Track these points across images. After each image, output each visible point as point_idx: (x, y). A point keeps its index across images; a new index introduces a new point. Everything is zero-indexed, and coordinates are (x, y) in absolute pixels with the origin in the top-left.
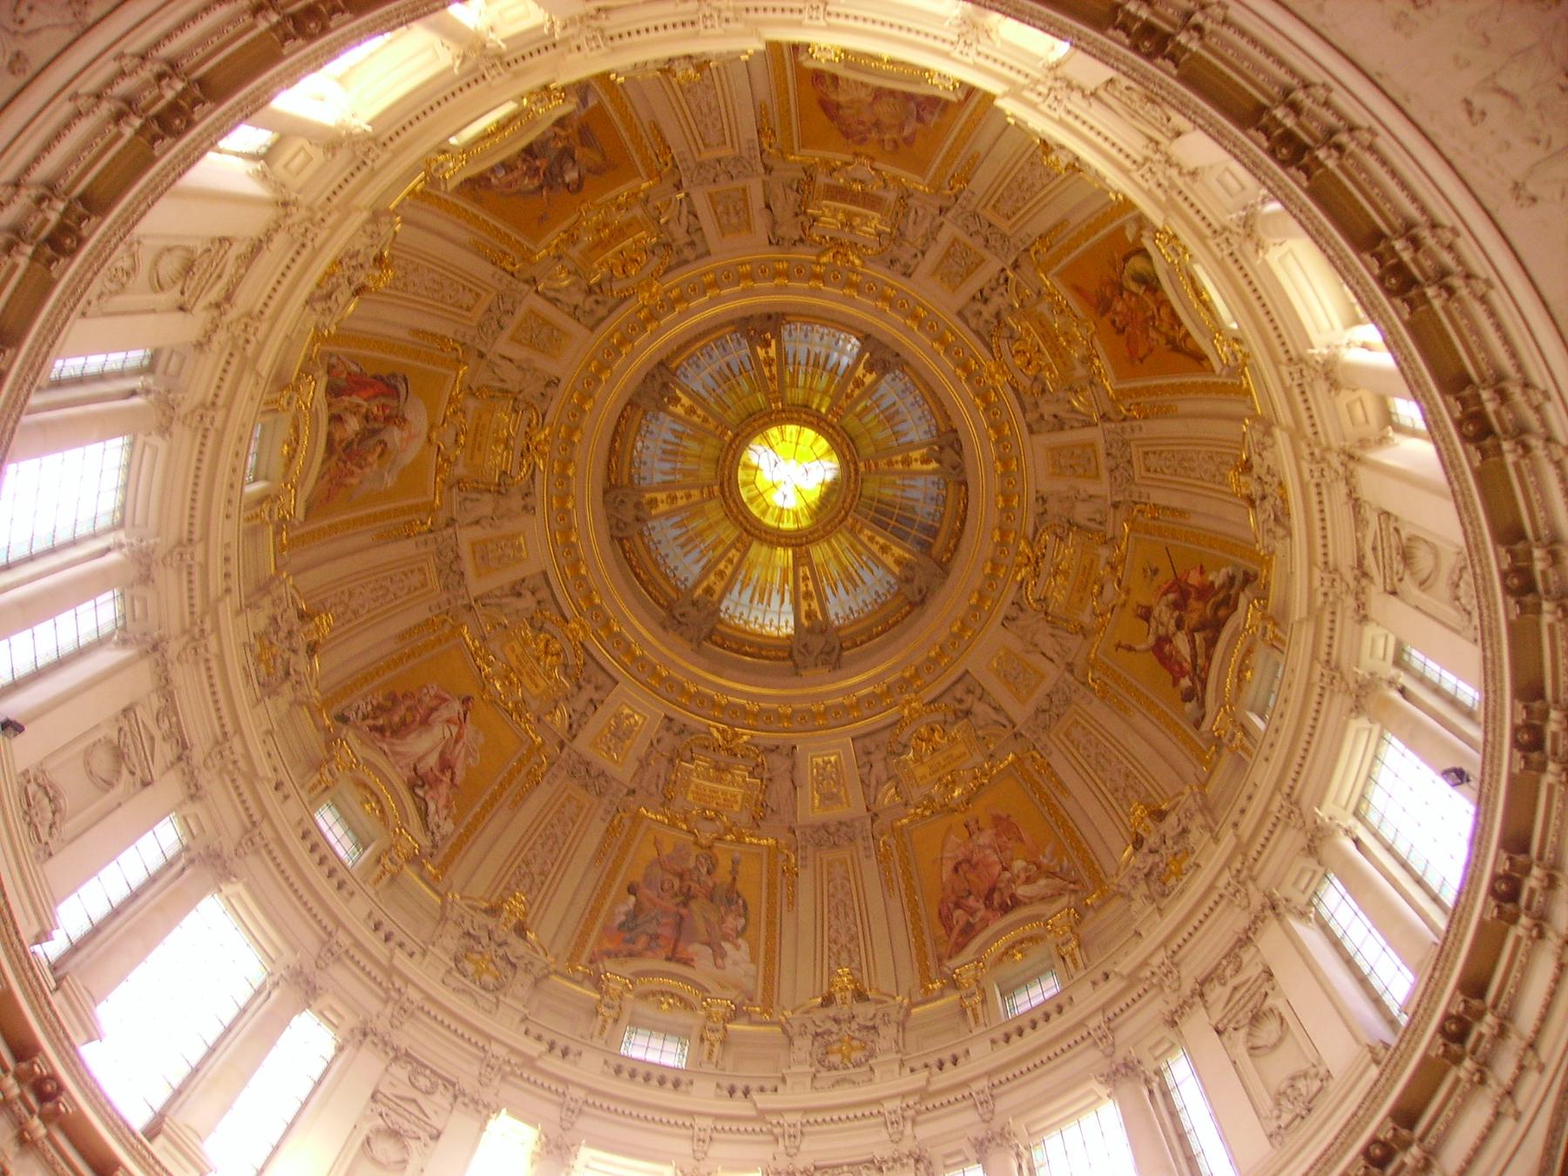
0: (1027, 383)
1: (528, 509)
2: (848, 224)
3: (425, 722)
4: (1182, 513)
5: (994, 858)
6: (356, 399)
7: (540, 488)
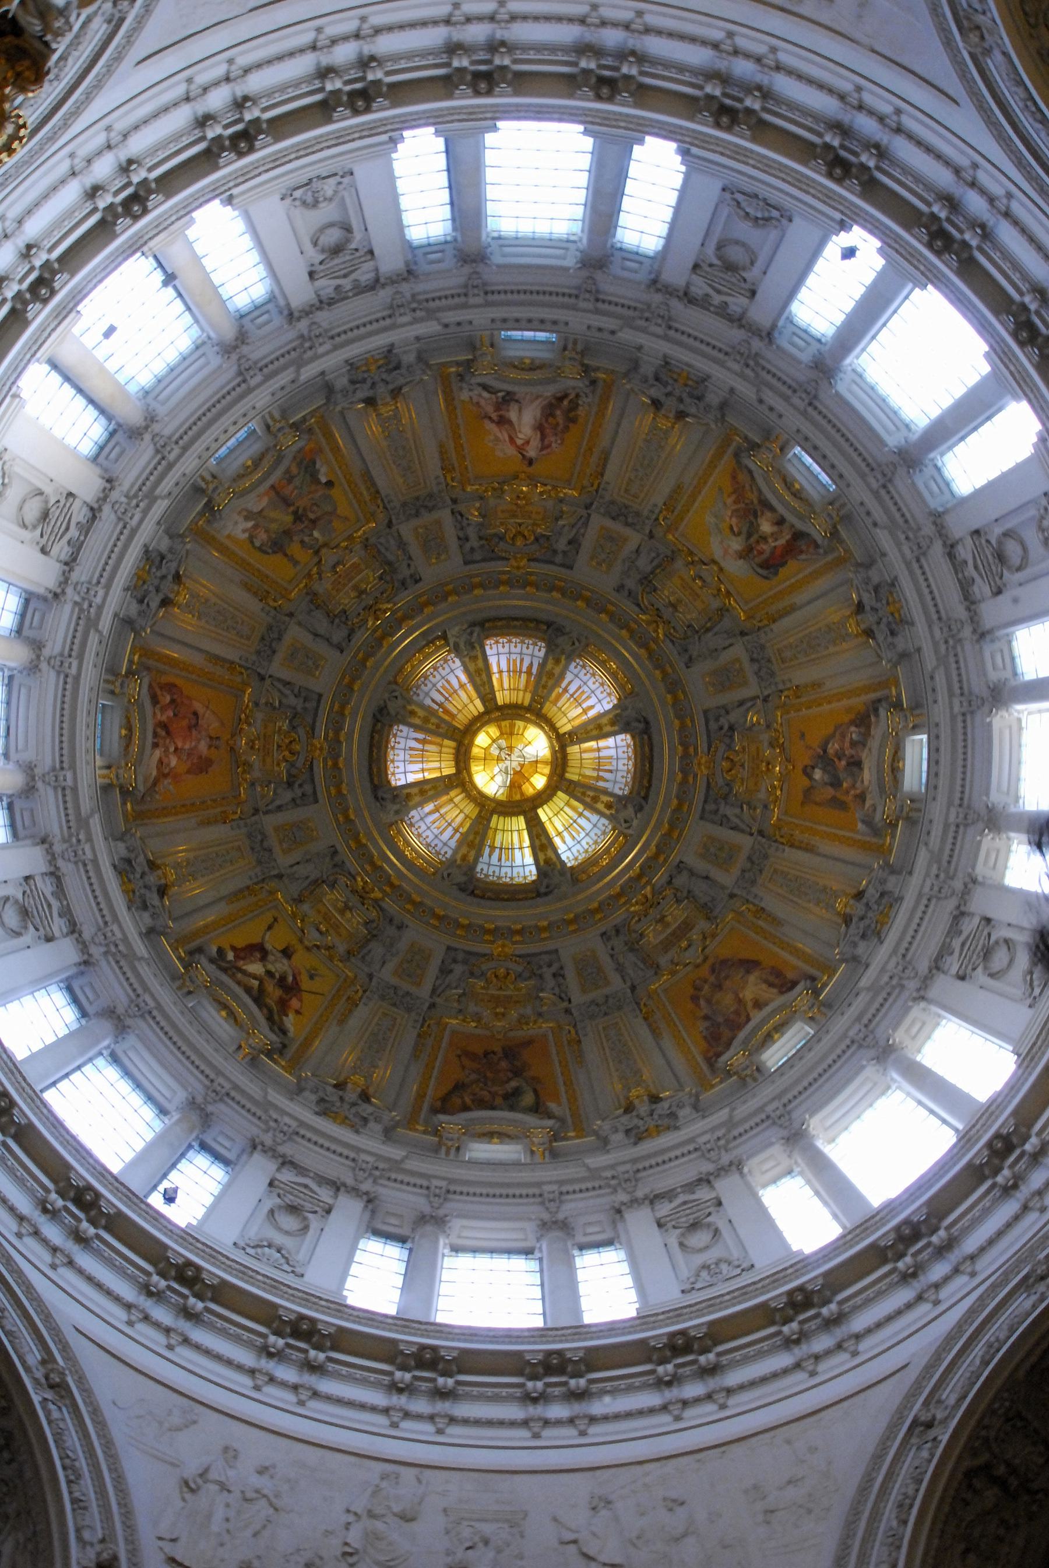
0: (484, 967)
1: (620, 588)
2: (661, 920)
3: (540, 428)
4: (342, 1022)
5: (187, 747)
6: (782, 542)
7: (628, 607)
